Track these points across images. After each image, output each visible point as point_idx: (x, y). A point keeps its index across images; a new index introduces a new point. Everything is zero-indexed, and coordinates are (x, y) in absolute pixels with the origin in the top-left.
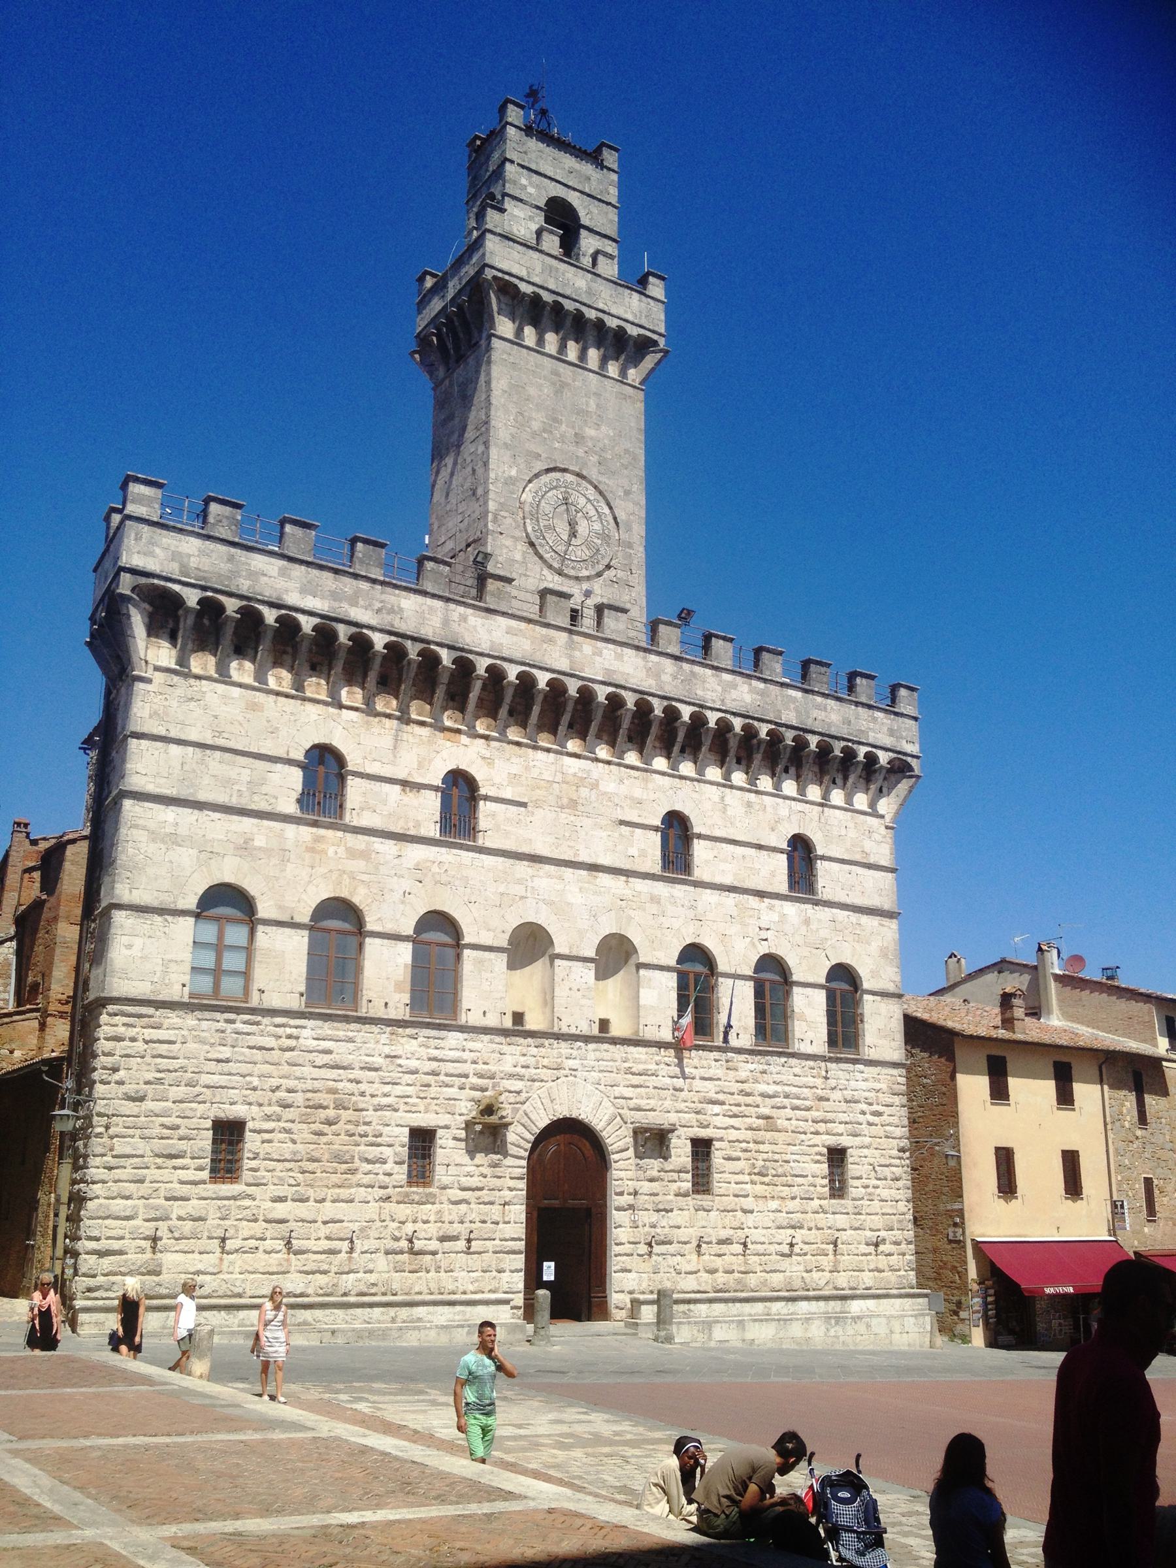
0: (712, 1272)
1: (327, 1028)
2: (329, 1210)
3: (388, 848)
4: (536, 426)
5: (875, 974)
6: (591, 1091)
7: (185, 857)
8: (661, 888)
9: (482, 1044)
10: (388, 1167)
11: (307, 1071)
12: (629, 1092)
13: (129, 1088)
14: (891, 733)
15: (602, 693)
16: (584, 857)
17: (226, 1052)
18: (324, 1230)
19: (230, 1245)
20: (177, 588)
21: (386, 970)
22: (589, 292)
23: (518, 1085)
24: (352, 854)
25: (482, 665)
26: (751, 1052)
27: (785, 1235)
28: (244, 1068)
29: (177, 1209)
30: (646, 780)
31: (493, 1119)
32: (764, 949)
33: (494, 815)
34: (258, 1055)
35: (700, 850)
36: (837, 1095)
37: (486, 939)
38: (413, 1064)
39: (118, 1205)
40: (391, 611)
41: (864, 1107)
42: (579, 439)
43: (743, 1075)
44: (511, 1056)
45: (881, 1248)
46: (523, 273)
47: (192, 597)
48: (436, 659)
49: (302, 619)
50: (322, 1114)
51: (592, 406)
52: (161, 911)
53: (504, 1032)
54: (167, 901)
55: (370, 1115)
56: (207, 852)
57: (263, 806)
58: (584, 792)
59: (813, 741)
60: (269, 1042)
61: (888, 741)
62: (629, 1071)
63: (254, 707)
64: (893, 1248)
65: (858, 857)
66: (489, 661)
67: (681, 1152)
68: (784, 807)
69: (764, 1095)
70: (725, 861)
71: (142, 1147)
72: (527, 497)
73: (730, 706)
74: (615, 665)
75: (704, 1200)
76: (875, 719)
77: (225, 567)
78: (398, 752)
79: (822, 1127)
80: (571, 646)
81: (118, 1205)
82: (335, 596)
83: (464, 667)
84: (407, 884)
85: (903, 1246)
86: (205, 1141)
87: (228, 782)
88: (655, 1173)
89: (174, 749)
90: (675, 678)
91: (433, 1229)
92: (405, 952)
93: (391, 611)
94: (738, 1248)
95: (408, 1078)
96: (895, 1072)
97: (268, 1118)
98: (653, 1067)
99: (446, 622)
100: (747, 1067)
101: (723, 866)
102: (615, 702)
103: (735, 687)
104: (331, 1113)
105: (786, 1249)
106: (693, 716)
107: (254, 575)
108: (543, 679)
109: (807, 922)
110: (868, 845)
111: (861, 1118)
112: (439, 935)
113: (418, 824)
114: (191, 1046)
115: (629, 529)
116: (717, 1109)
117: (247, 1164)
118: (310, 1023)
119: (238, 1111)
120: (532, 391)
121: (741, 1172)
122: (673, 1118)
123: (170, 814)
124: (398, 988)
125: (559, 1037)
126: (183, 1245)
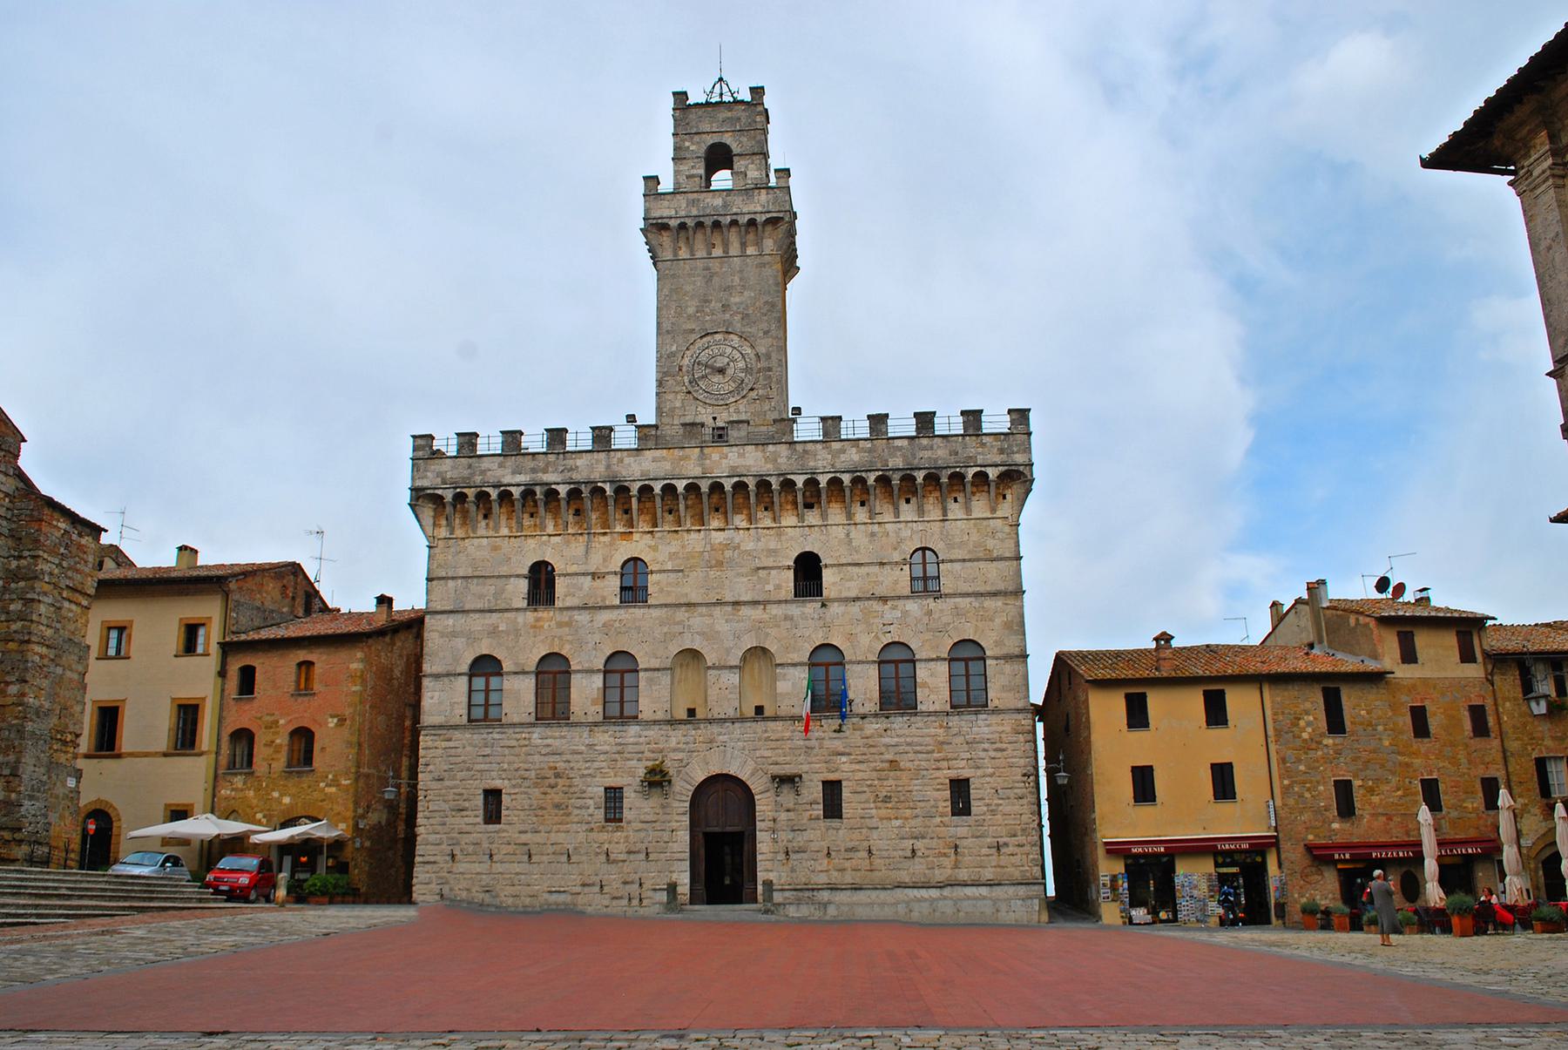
0: (843, 870)
1: (548, 732)
2: (554, 837)
3: (582, 618)
4: (691, 310)
5: (997, 643)
6: (738, 755)
7: (460, 642)
8: (795, 610)
9: (653, 733)
10: (591, 811)
11: (537, 758)
12: (768, 753)
13: (436, 775)
14: (1001, 451)
15: (728, 485)
16: (729, 598)
17: (488, 751)
18: (551, 849)
19: (495, 858)
20: (439, 492)
21: (585, 691)
22: (725, 205)
23: (680, 756)
24: (560, 625)
25: (635, 488)
26: (876, 715)
27: (908, 844)
28: (499, 759)
29: (466, 839)
30: (779, 535)
31: (658, 778)
32: (887, 639)
33: (658, 583)
34: (507, 751)
35: (828, 576)
36: (960, 739)
37: (655, 663)
38: (606, 748)
39: (432, 838)
40: (571, 469)
41: (986, 746)
42: (726, 307)
43: (868, 732)
44: (676, 737)
45: (1003, 850)
46: (673, 213)
47: (448, 495)
48: (604, 491)
49: (513, 489)
50: (547, 782)
51: (737, 279)
52: (448, 675)
53: (672, 722)
54: (451, 669)
55: (576, 781)
56: (472, 638)
57: (503, 606)
58: (728, 554)
59: (920, 476)
60: (514, 743)
61: (998, 459)
62: (768, 739)
63: (495, 548)
64: (1017, 850)
65: (981, 555)
66: (639, 484)
67: (813, 791)
68: (906, 533)
69: (887, 746)
70: (851, 579)
71: (445, 806)
72: (686, 361)
73: (839, 466)
74: (740, 462)
75: (835, 823)
76: (983, 445)
77: (466, 473)
78: (586, 557)
79: (945, 764)
80: (703, 456)
81: (432, 838)
82: (534, 471)
83: (622, 490)
84: (597, 638)
85: (1027, 848)
86: (479, 801)
87: (481, 596)
88: (791, 805)
89: (451, 583)
90: (789, 458)
91: (622, 847)
92: (598, 681)
93: (571, 469)
94: (865, 854)
95: (602, 757)
96: (1020, 716)
97: (514, 786)
98: (788, 734)
99: (608, 467)
100: (872, 727)
101: (848, 584)
102: (740, 487)
103: (843, 451)
104: (552, 781)
105: (909, 854)
106: (807, 483)
107: (483, 472)
108: (681, 485)
109: (930, 613)
110: (990, 543)
111: (982, 754)
112: (620, 667)
113: (604, 599)
114: (469, 748)
115: (768, 356)
116: (844, 759)
117: (504, 812)
118: (538, 730)
119: (497, 784)
120: (688, 288)
121: (867, 801)
122: (805, 768)
123: (450, 621)
124: (594, 703)
125: (710, 721)
126: (469, 858)
